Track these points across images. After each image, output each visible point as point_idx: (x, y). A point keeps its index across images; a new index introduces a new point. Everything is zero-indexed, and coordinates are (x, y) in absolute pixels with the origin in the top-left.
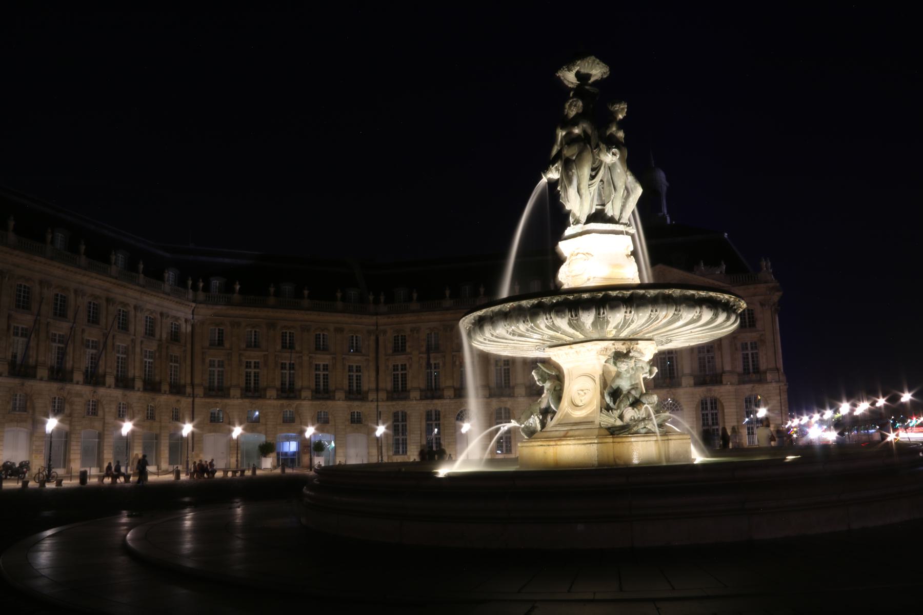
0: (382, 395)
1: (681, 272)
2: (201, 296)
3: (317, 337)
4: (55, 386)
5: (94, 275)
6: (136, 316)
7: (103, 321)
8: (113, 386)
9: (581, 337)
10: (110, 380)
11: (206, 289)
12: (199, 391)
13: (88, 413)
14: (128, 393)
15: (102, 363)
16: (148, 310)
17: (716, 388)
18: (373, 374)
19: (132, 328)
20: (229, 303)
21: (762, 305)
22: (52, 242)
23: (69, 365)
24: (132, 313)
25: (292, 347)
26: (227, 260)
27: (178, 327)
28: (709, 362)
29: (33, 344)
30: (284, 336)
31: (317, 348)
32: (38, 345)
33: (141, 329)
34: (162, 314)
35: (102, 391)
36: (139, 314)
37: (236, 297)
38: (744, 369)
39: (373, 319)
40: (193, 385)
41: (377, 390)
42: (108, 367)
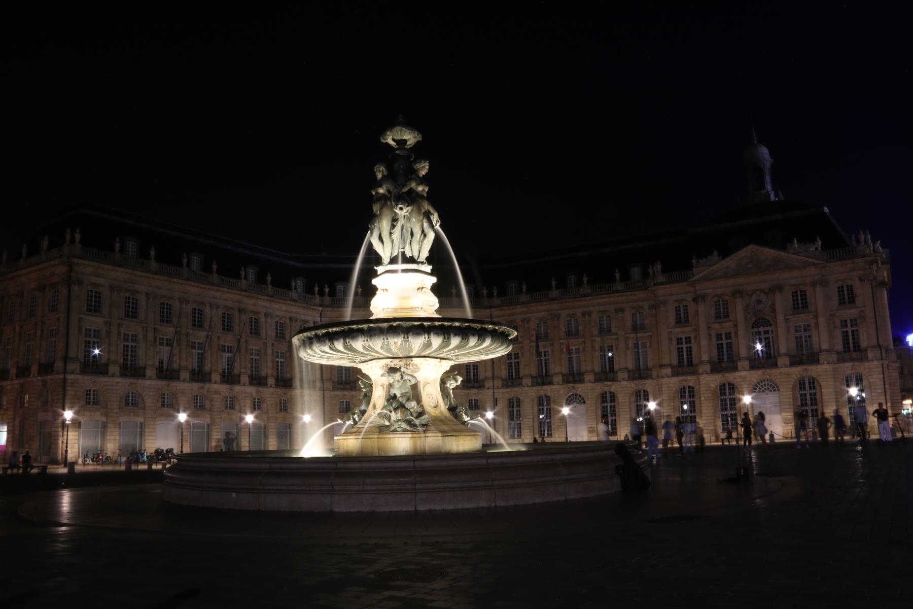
0: (498, 383)
1: (773, 251)
2: (327, 300)
4: (196, 386)
5: (225, 290)
6: (266, 323)
7: (236, 328)
8: (247, 383)
9: (390, 355)
10: (245, 379)
13: (226, 408)
14: (261, 389)
15: (236, 365)
16: (278, 316)
17: (813, 367)
19: (263, 333)
21: (861, 280)
22: (188, 265)
23: (207, 368)
24: (263, 319)
28: (806, 341)
29: (176, 352)
32: (180, 352)
33: (272, 333)
34: (291, 319)
35: (237, 388)
36: (269, 320)
38: (844, 347)
41: (493, 378)
42: (242, 368)
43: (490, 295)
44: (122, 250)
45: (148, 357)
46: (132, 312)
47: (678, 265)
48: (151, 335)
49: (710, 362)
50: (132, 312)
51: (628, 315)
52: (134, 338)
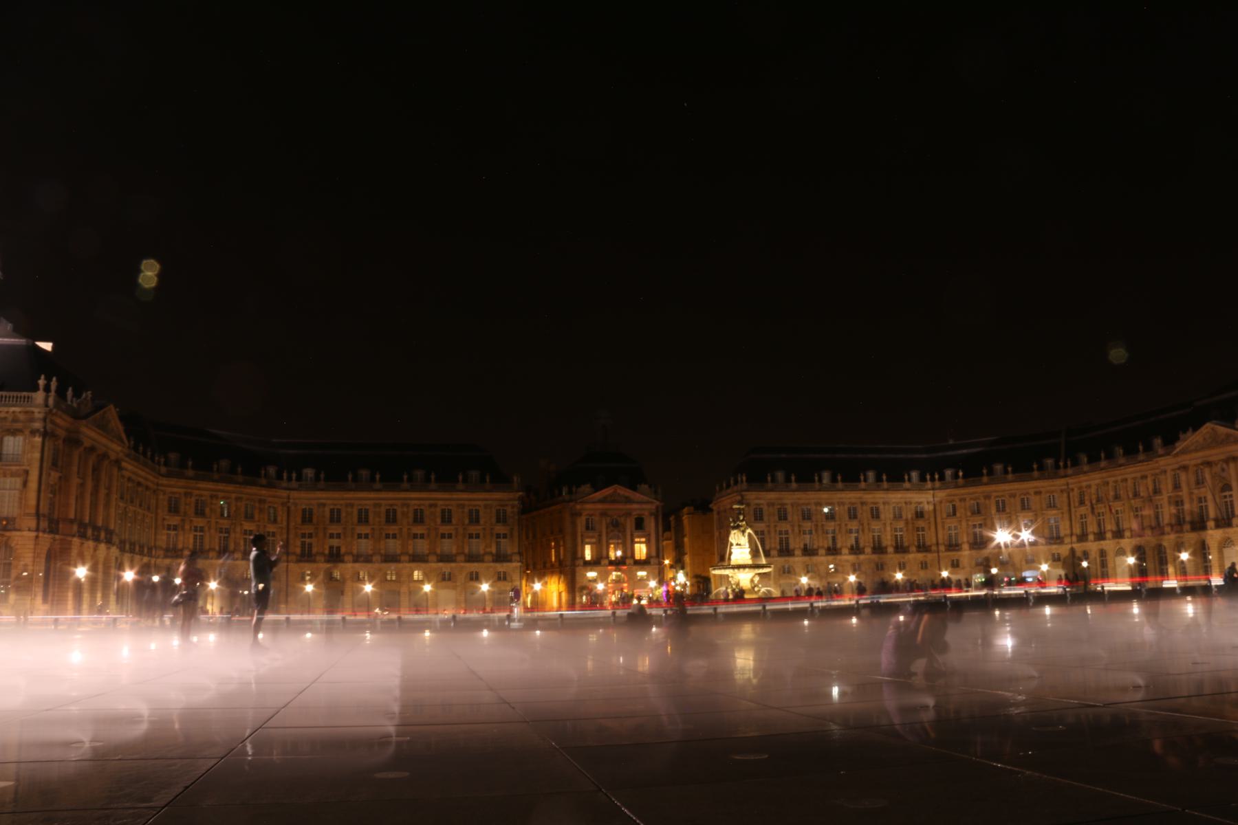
0: (1074, 538)
2: (937, 484)
3: (1023, 500)
11: (942, 478)
12: (942, 548)
18: (1068, 523)
19: (882, 516)
20: (957, 487)
22: (820, 480)
23: (839, 545)
24: (881, 507)
25: (1004, 510)
30: (997, 502)
37: (960, 481)
39: (1063, 481)
41: (1072, 535)
43: (1066, 467)
45: (796, 543)
46: (783, 517)
47: (1170, 441)
48: (796, 529)
50: (783, 517)
51: (1149, 481)
52: (787, 532)
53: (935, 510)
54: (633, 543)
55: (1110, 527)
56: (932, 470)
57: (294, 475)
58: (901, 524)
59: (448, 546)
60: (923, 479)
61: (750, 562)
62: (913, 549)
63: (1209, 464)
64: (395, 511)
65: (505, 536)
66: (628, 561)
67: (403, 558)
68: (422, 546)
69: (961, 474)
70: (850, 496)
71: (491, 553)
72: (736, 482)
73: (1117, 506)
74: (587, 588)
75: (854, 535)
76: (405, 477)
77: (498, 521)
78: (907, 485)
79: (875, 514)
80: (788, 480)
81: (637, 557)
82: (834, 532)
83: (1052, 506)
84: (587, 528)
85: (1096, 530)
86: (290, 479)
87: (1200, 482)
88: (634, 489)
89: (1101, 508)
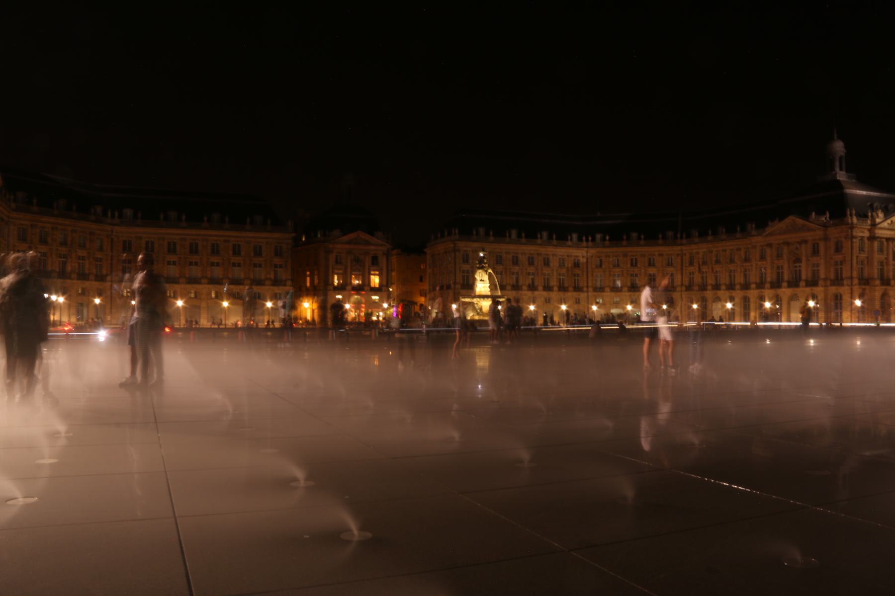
0: (684, 288)
2: (590, 244)
3: (650, 259)
10: (540, 288)
11: (594, 240)
12: (591, 289)
14: (551, 293)
17: (814, 288)
19: (551, 264)
20: (604, 247)
22: (510, 236)
23: (520, 283)
24: (551, 257)
25: (636, 265)
26: (609, 222)
27: (578, 261)
30: (632, 260)
31: (650, 265)
35: (536, 293)
37: (607, 243)
39: (679, 248)
40: (587, 287)
42: (539, 282)
43: (681, 238)
44: (477, 234)
47: (762, 225)
49: (771, 283)
51: (742, 253)
53: (587, 262)
54: (370, 274)
55: (711, 281)
56: (587, 234)
57: (116, 214)
58: (564, 271)
59: (238, 273)
60: (580, 239)
61: (489, 293)
62: (571, 289)
63: (787, 244)
64: (197, 245)
65: (281, 266)
66: (366, 288)
67: (203, 281)
68: (218, 272)
69: (607, 238)
70: (530, 249)
71: (270, 279)
72: (450, 234)
73: (718, 268)
74: (339, 306)
75: (531, 277)
76: (205, 218)
77: (276, 254)
78: (569, 243)
79: (547, 263)
80: (487, 234)
81: (372, 285)
82: (517, 273)
83: (670, 264)
84: (337, 262)
85: (714, 283)
86: (113, 216)
87: (779, 256)
88: (371, 233)
89: (704, 268)
